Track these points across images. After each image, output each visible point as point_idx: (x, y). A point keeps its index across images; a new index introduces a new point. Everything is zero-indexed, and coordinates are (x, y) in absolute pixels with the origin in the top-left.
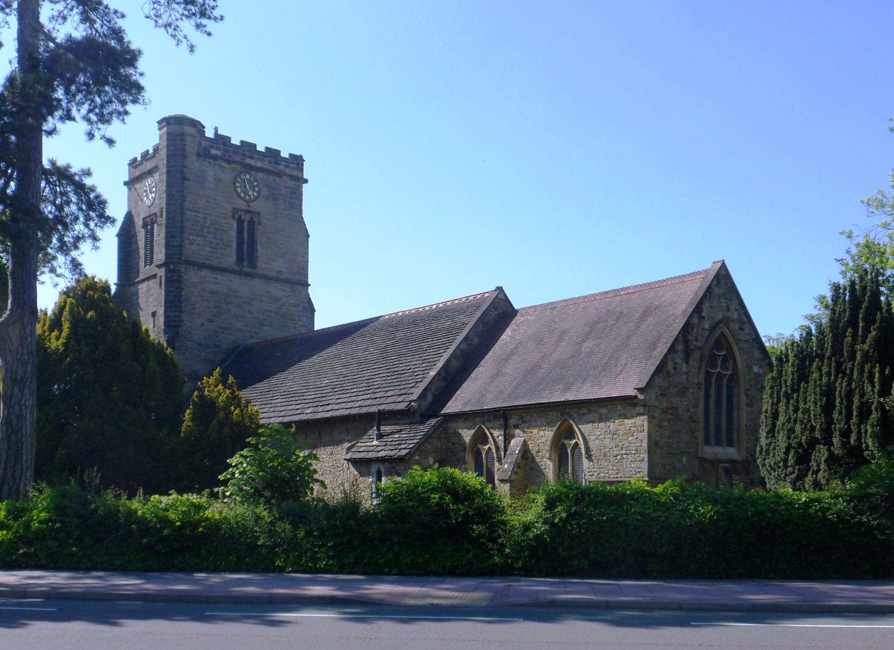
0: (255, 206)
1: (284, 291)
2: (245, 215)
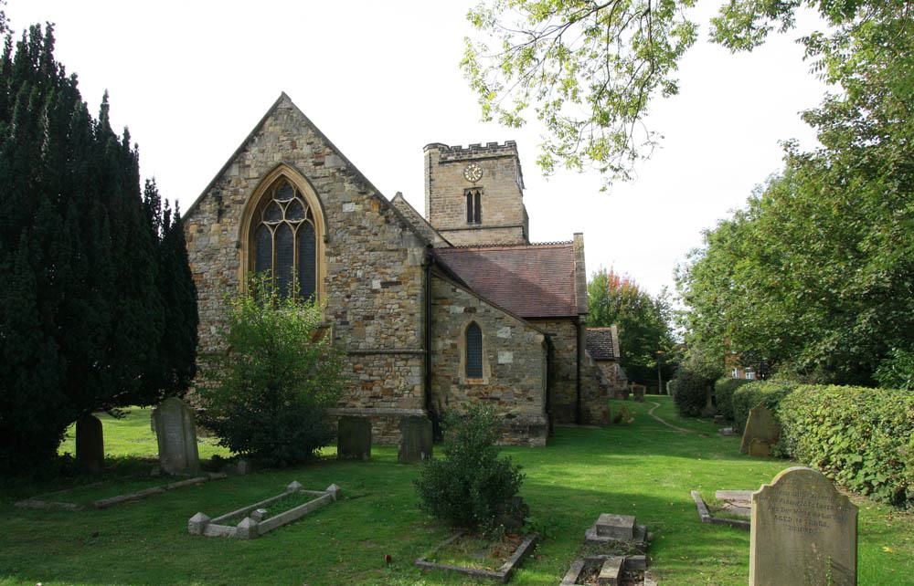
0: (479, 184)
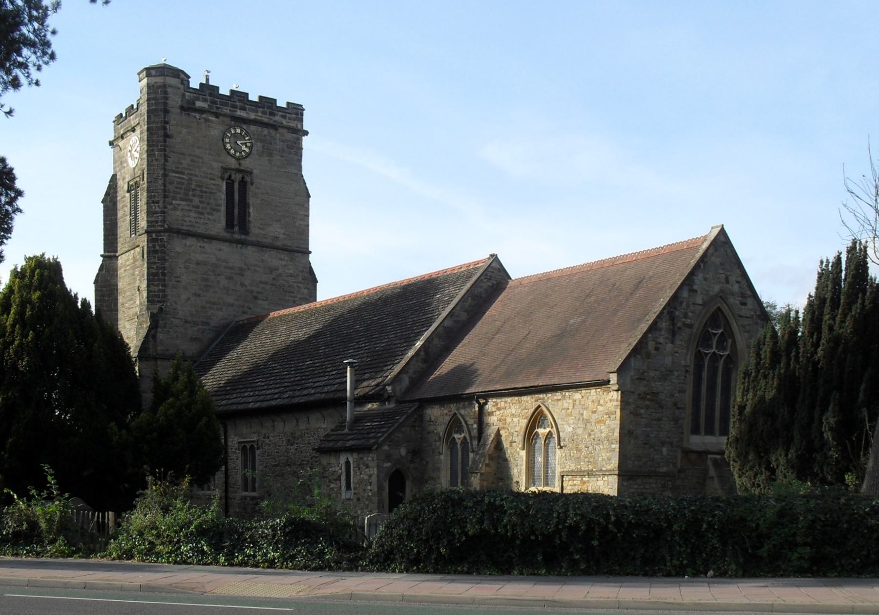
1: (281, 259)
2: (235, 174)
